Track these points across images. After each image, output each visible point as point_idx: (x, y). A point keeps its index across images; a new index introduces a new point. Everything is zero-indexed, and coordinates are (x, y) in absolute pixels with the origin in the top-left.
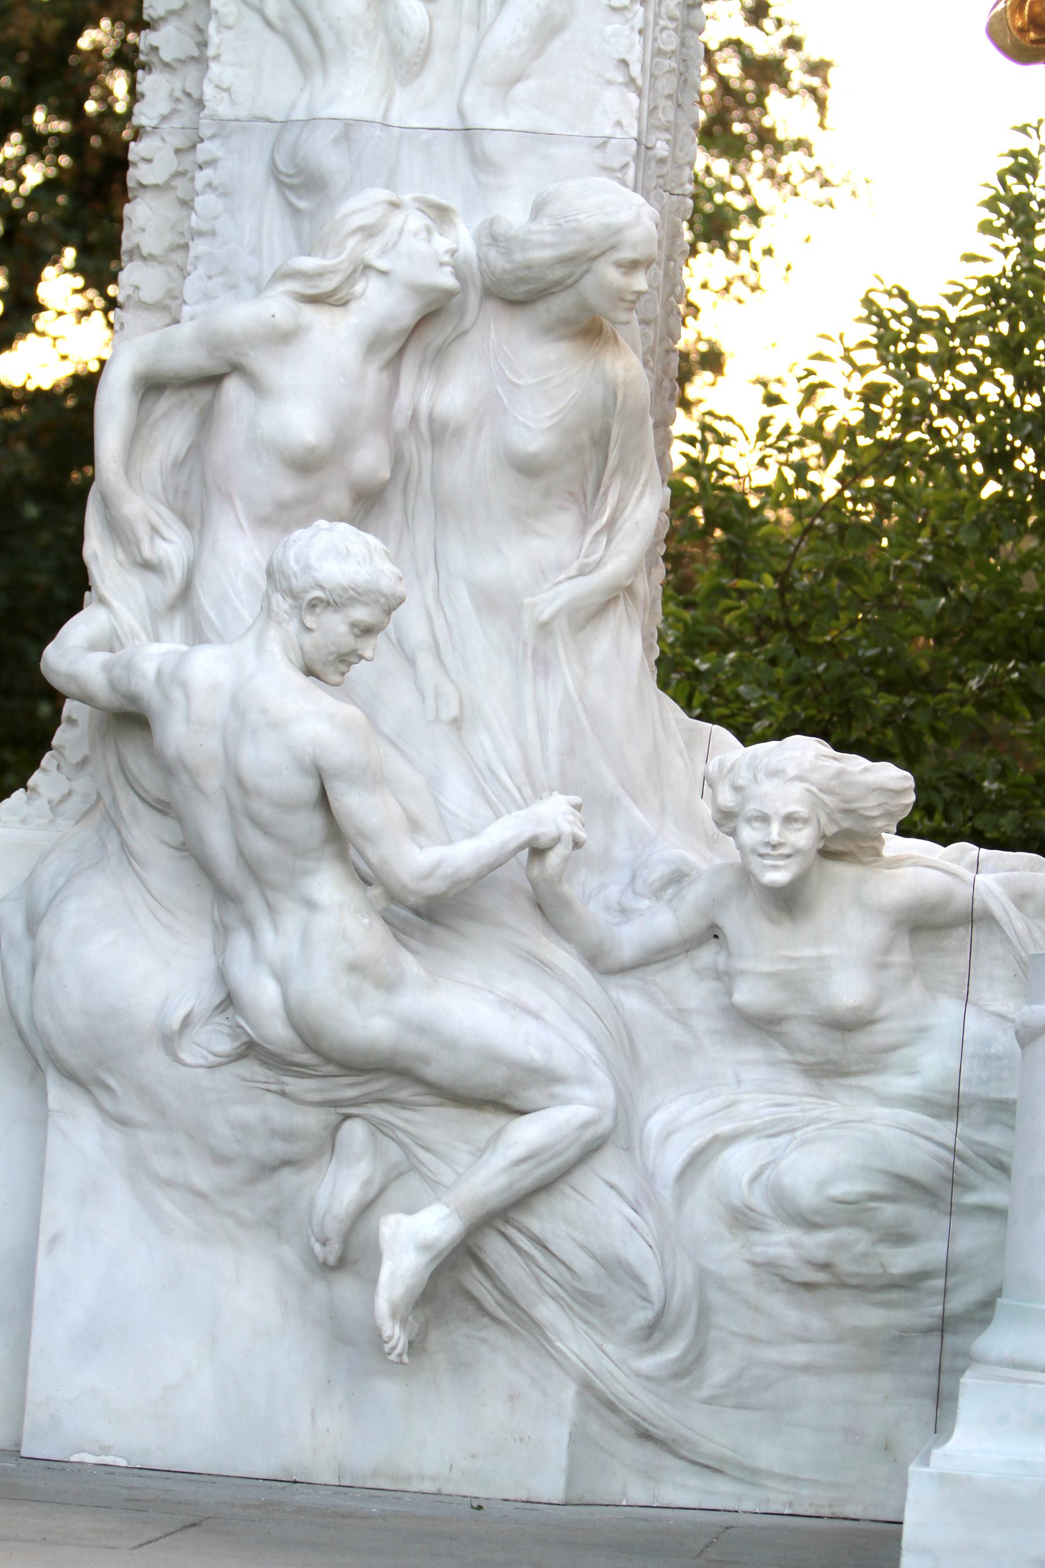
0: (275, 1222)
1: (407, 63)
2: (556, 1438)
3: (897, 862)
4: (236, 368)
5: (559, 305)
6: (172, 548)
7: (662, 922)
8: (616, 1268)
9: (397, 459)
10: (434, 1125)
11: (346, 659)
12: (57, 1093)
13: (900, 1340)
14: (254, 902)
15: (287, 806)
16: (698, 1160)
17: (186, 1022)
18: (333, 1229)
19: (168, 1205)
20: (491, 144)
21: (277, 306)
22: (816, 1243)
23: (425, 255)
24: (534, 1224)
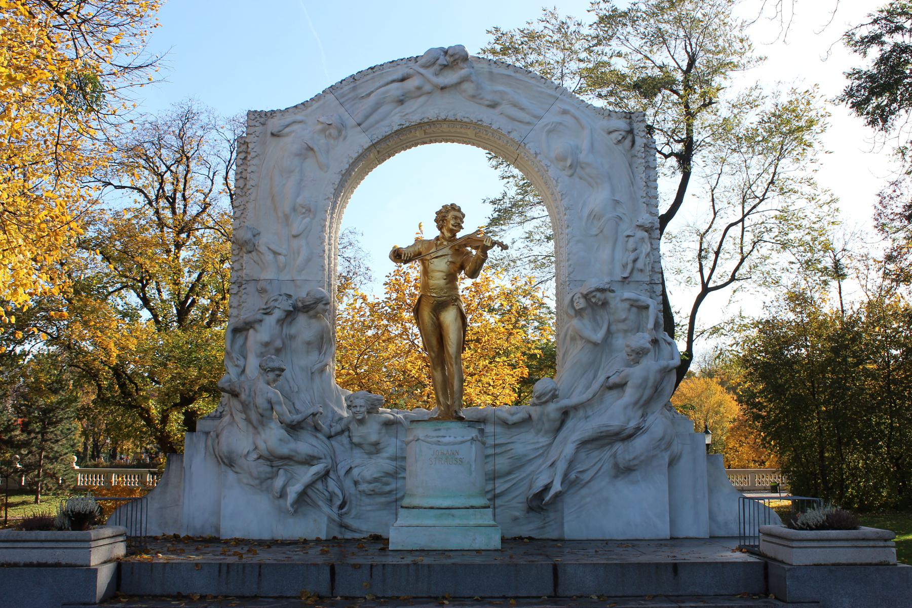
0: (269, 490)
1: (280, 269)
3: (382, 413)
4: (251, 327)
5: (312, 313)
7: (338, 428)
9: (284, 343)
13: (388, 504)
14: (260, 428)
15: (266, 410)
17: (248, 452)
18: (279, 490)
20: (298, 282)
22: (371, 486)
23: (287, 305)
24: (317, 487)
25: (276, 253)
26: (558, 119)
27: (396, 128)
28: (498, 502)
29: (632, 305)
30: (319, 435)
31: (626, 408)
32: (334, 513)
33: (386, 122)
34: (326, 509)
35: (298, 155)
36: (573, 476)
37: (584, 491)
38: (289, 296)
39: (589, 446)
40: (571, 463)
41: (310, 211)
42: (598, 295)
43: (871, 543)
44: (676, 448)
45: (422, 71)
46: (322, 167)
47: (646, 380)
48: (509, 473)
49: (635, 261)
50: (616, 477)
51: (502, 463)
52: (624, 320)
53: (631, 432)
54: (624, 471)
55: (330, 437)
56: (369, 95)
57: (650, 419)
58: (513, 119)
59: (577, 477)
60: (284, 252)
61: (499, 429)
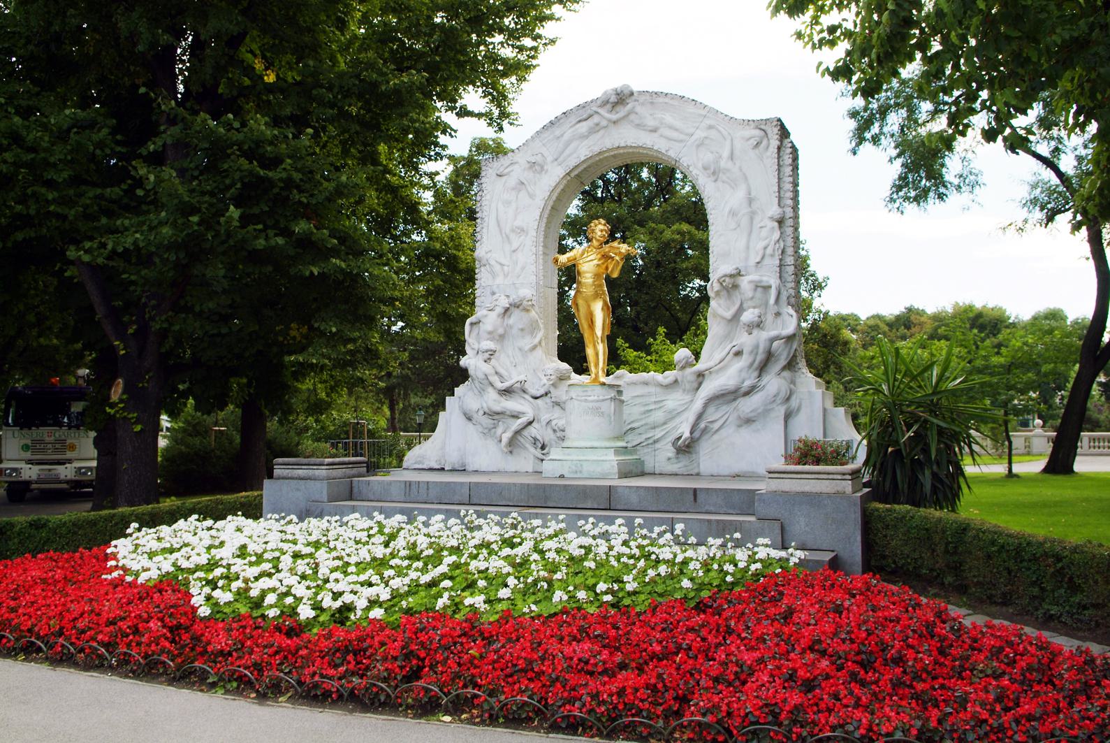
1: (506, 276)
2: (531, 462)
6: (476, 346)
7: (542, 391)
8: (535, 439)
9: (505, 331)
10: (511, 420)
11: (490, 359)
12: (467, 422)
16: (549, 423)
19: (481, 435)
21: (485, 312)
23: (504, 303)
25: (502, 265)
26: (703, 134)
27: (583, 159)
28: (657, 446)
29: (757, 286)
30: (527, 397)
31: (741, 371)
32: (538, 453)
33: (575, 155)
34: (532, 450)
35: (513, 189)
36: (702, 425)
37: (716, 437)
38: (508, 296)
39: (717, 402)
40: (700, 417)
41: (523, 230)
42: (727, 279)
43: (831, 476)
44: (794, 403)
45: (599, 110)
46: (532, 196)
47: (757, 347)
48: (665, 423)
49: (765, 248)
50: (740, 426)
51: (658, 416)
52: (752, 298)
53: (747, 389)
54: (748, 421)
55: (536, 398)
56: (562, 135)
57: (766, 379)
58: (670, 139)
59: (706, 427)
60: (507, 263)
61: (659, 390)
